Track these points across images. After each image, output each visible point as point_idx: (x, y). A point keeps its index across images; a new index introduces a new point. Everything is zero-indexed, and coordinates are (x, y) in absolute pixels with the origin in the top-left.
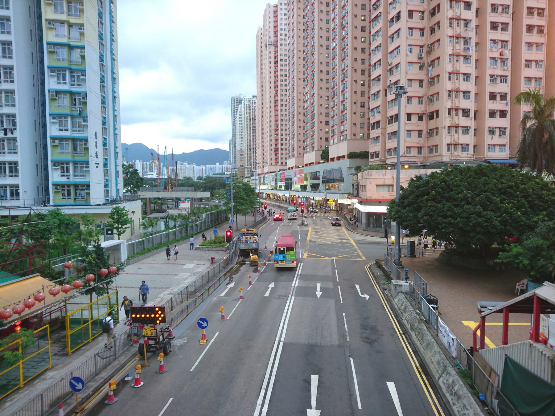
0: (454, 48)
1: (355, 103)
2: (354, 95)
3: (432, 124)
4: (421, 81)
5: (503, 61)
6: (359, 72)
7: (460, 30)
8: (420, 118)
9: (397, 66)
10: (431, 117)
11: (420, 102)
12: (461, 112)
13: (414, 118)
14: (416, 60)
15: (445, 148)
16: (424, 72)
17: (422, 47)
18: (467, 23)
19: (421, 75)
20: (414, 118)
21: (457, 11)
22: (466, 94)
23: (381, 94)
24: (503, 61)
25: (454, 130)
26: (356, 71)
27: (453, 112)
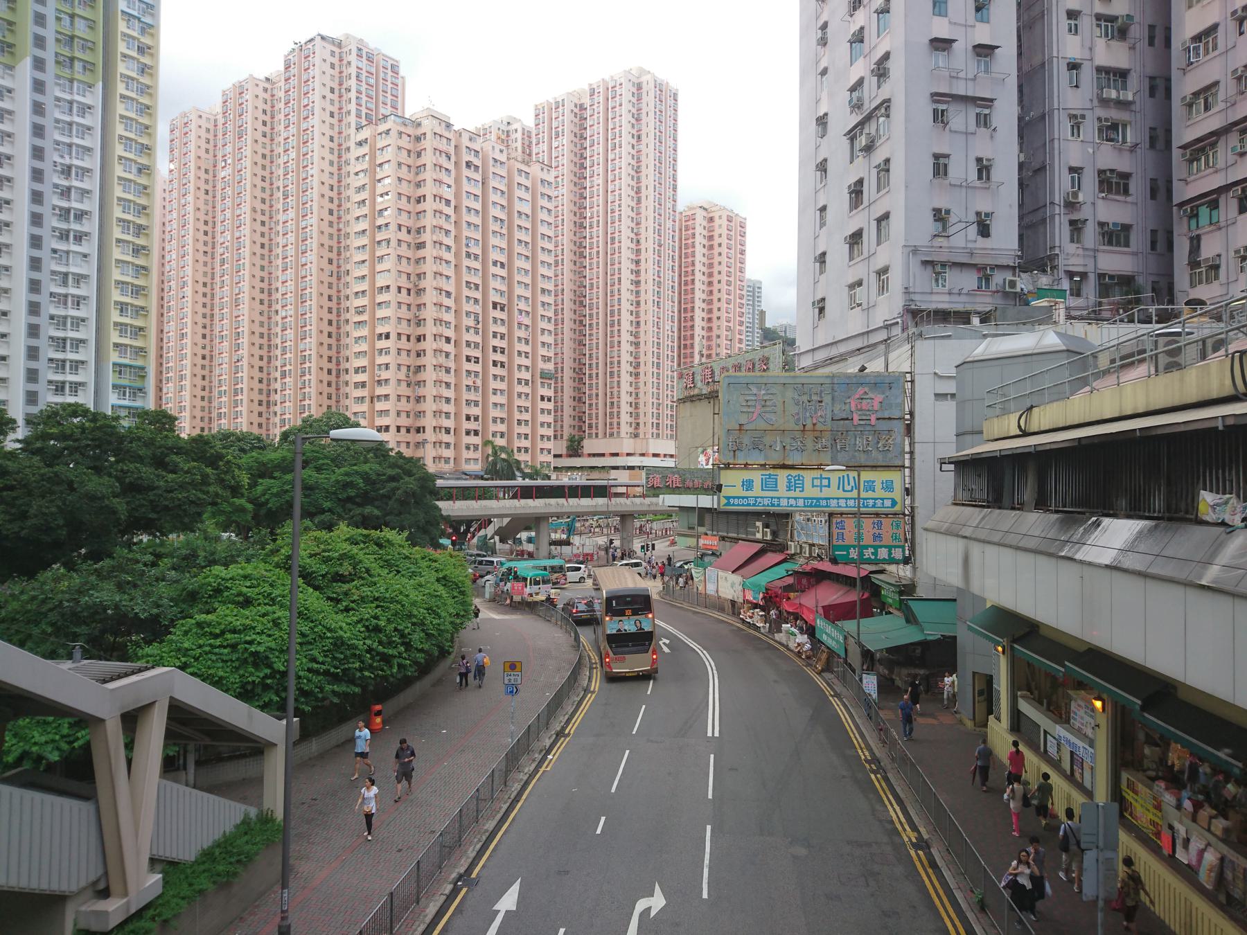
0: (438, 376)
1: (321, 393)
2: (320, 385)
3: (420, 437)
4: (409, 397)
5: (476, 389)
6: (325, 358)
7: (442, 360)
8: (408, 431)
9: (386, 380)
10: (418, 431)
11: (408, 416)
12: (443, 430)
13: (403, 431)
14: (404, 378)
15: (431, 460)
16: (411, 389)
17: (409, 367)
18: (447, 354)
19: (408, 392)
20: (403, 431)
21: (440, 343)
22: (447, 415)
23: (367, 400)
24: (476, 389)
25: (438, 445)
26: (321, 356)
27: (438, 430)
